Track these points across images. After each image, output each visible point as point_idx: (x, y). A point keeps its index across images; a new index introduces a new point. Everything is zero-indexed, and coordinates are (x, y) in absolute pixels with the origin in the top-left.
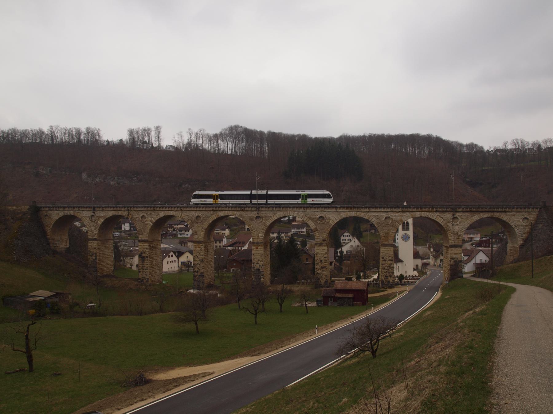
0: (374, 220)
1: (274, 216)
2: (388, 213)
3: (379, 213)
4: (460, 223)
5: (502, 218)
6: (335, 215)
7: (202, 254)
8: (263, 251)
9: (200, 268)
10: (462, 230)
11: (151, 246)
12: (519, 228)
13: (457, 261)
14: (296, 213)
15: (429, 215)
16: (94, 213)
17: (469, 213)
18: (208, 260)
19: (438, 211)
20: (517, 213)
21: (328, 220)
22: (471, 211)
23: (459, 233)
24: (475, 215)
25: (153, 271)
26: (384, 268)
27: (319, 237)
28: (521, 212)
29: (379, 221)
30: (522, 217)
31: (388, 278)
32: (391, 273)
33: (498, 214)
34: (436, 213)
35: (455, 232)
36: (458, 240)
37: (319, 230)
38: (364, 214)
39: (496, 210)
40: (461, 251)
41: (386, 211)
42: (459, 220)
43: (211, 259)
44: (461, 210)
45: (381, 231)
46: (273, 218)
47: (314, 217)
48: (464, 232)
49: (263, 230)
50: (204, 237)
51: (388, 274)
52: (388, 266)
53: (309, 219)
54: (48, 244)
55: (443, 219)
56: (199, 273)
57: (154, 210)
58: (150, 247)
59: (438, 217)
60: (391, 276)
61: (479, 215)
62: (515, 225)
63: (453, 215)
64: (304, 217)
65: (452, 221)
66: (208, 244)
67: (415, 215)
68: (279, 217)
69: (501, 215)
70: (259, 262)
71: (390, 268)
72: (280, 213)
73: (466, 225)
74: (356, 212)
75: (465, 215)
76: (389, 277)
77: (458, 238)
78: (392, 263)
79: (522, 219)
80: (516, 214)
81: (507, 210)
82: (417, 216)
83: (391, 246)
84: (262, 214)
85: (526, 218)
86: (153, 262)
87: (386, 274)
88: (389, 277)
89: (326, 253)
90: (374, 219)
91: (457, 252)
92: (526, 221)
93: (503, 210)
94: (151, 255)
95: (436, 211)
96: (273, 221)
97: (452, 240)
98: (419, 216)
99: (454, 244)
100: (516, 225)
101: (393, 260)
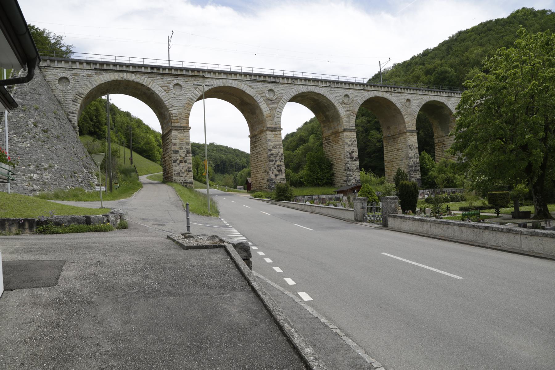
66: (443, 138)
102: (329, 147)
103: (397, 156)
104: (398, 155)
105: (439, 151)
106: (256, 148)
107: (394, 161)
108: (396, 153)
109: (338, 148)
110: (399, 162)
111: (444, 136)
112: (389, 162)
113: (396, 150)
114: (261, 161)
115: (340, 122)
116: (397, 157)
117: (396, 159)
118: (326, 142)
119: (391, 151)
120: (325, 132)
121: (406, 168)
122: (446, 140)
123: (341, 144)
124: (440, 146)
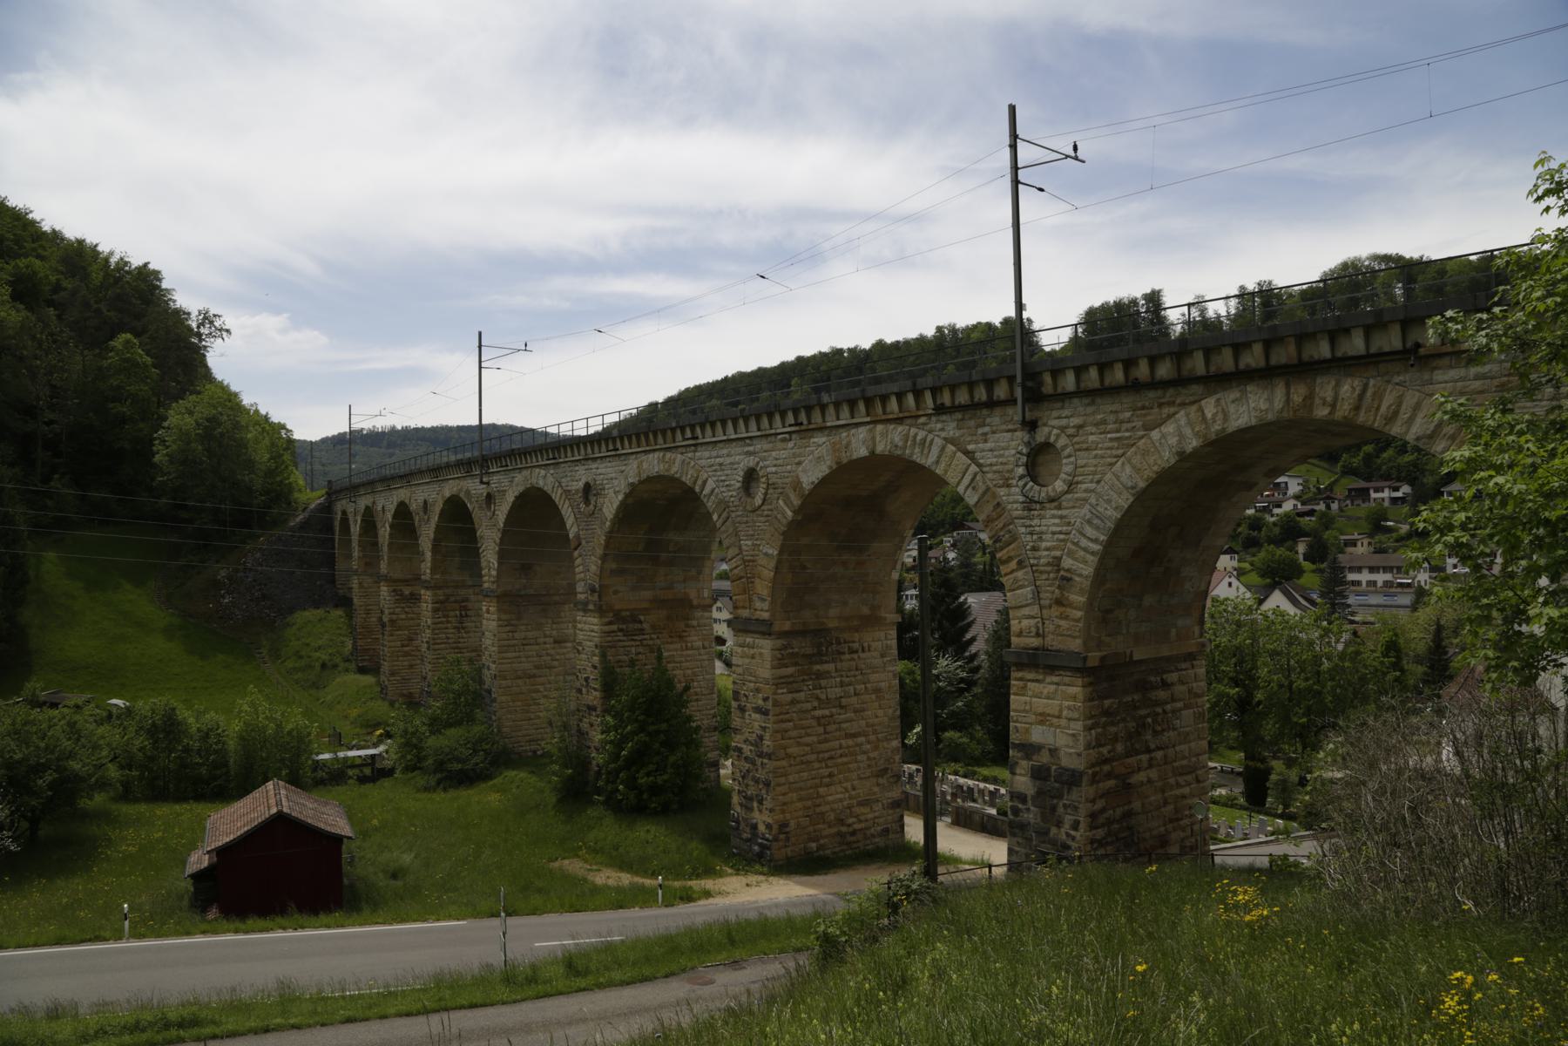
2: (751, 449)
3: (725, 451)
4: (1071, 486)
5: (1392, 417)
6: (613, 475)
8: (494, 623)
10: (1084, 542)
11: (407, 593)
14: (543, 472)
15: (907, 436)
17: (1128, 399)
22: (1134, 386)
23: (1067, 563)
24: (1166, 411)
25: (411, 666)
26: (739, 750)
31: (750, 809)
33: (1348, 388)
34: (939, 426)
35: (1044, 557)
36: (1061, 617)
37: (583, 542)
38: (684, 461)
39: (1323, 350)
40: (1074, 698)
48: (1093, 553)
50: (434, 569)
52: (752, 745)
53: (564, 497)
54: (333, 582)
55: (980, 465)
58: (401, 595)
59: (951, 448)
60: (761, 802)
61: (1194, 408)
63: (1031, 426)
65: (1021, 471)
66: (462, 592)
67: (848, 445)
68: (516, 493)
69: (1378, 396)
71: (759, 756)
72: (519, 477)
73: (1109, 501)
74: (662, 454)
75: (1104, 422)
77: (1059, 602)
78: (764, 729)
82: (854, 457)
86: (411, 640)
87: (747, 785)
88: (755, 804)
90: (707, 491)
91: (1052, 706)
94: (402, 619)
95: (940, 410)
97: (1026, 611)
98: (863, 452)
99: (1035, 642)
101: (765, 713)
102: (633, 650)
104: (558, 657)
105: (447, 628)
106: (824, 683)
107: (540, 676)
108: (552, 652)
109: (682, 656)
110: (561, 678)
111: (470, 586)
112: (520, 678)
113: (547, 640)
114: (854, 736)
115: (700, 573)
116: (556, 663)
117: (550, 668)
118: (621, 630)
119: (532, 641)
120: (616, 592)
122: (472, 597)
123: (700, 644)
124: (452, 613)
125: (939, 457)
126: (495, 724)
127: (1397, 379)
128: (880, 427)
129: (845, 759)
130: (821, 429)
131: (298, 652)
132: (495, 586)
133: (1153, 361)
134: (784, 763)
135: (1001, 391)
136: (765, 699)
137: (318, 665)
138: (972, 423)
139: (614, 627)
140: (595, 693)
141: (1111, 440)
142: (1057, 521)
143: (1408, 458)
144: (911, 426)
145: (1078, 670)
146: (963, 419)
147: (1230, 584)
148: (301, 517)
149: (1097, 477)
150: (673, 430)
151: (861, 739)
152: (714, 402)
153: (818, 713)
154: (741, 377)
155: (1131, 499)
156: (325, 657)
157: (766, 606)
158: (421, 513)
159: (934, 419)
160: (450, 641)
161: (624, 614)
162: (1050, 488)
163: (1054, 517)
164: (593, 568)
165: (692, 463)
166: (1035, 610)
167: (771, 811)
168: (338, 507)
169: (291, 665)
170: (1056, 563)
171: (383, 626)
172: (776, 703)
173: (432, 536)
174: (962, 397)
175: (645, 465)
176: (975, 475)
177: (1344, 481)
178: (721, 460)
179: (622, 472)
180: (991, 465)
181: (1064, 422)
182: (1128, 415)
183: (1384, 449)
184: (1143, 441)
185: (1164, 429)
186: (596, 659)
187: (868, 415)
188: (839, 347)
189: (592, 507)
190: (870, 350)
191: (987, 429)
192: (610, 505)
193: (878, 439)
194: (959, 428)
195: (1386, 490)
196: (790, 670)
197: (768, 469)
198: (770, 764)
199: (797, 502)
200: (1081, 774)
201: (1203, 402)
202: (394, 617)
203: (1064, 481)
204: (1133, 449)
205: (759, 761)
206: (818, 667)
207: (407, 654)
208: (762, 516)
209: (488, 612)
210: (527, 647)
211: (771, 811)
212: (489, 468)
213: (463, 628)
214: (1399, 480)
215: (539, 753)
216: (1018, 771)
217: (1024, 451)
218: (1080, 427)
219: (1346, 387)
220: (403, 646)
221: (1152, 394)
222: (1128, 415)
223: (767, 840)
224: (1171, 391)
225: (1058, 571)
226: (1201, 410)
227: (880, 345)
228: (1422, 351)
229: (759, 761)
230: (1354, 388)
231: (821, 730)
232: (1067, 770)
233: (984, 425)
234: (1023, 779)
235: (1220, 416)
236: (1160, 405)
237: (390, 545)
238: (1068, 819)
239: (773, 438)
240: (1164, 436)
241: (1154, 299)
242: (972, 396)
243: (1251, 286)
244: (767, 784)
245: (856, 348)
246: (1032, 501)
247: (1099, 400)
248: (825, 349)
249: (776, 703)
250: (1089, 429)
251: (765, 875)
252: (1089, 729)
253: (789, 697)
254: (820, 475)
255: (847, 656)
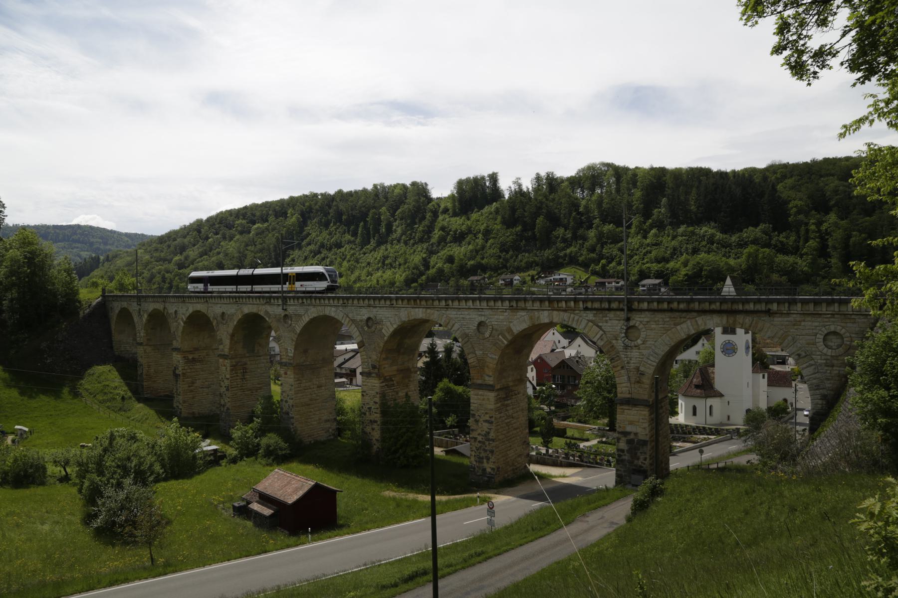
0: (456, 329)
1: (306, 315)
2: (483, 313)
3: (466, 313)
6: (390, 316)
7: (228, 376)
8: (292, 380)
9: (226, 401)
10: (649, 362)
11: (190, 358)
12: (812, 362)
13: (636, 440)
14: (333, 309)
15: (569, 317)
16: (140, 305)
17: (669, 314)
18: (243, 388)
19: (591, 309)
20: (809, 319)
21: (381, 326)
22: (671, 310)
23: (642, 369)
24: (682, 320)
25: (193, 398)
26: (476, 439)
27: (366, 360)
28: (821, 314)
29: (467, 331)
30: (824, 329)
32: (488, 452)
34: (585, 315)
35: (632, 366)
37: (366, 345)
39: (740, 307)
40: (645, 415)
41: (479, 309)
42: (643, 335)
43: (259, 384)
44: (645, 305)
45: (468, 354)
46: (304, 319)
47: (359, 318)
49: (292, 340)
50: (230, 349)
51: (483, 454)
53: (351, 322)
54: (112, 347)
55: (603, 331)
56: (225, 408)
57: (184, 302)
58: (188, 359)
59: (591, 324)
60: (488, 459)
61: (693, 320)
62: (798, 352)
64: (344, 318)
65: (623, 335)
67: (538, 318)
70: (288, 400)
74: (424, 310)
76: (485, 461)
77: (638, 382)
78: (491, 429)
79: (822, 337)
80: (804, 321)
81: (774, 307)
82: (542, 322)
83: (490, 390)
84: (291, 310)
85: (835, 333)
86: (193, 383)
88: (485, 461)
89: (377, 393)
90: (455, 328)
92: (834, 341)
93: (762, 307)
95: (586, 309)
96: (304, 324)
97: (624, 385)
98: (546, 321)
99: (629, 396)
100: (803, 354)
101: (491, 423)
102: (390, 394)
103: (317, 396)
105: (237, 379)
108: (316, 392)
114: (515, 429)
116: (318, 398)
117: (316, 400)
118: (386, 385)
120: (384, 368)
121: (331, 413)
122: (249, 363)
124: (239, 371)
125: (585, 327)
126: (292, 430)
127: (762, 319)
128: (555, 313)
129: (513, 439)
130: (523, 309)
131: (103, 390)
132: (292, 361)
133: (679, 303)
134: (497, 443)
135: (614, 305)
136: (491, 417)
137: (119, 398)
138: (601, 315)
139: (384, 384)
140: (376, 415)
141: (661, 327)
142: (638, 354)
143: (622, 267)
144: (571, 313)
145: (646, 406)
146: (596, 314)
147: (554, 334)
148: (88, 310)
149: (655, 340)
150: (433, 300)
151: (518, 430)
152: (240, 221)
153: (507, 421)
154: (255, 207)
155: (668, 348)
156: (122, 393)
157: (491, 379)
158: (219, 319)
159: (582, 312)
160: (239, 386)
161: (387, 378)
162: (635, 342)
163: (636, 352)
164: (374, 357)
165: (445, 316)
166: (629, 385)
167: (494, 463)
168: (117, 306)
169: (101, 398)
170: (638, 369)
171: (176, 376)
172: (495, 418)
173: (231, 331)
174: (597, 305)
175: (412, 313)
176: (602, 335)
177: (592, 277)
178: (464, 316)
179: (396, 315)
180: (609, 331)
181: (642, 319)
182: (668, 319)
183: (610, 262)
184: (673, 330)
185: (681, 325)
186: (377, 400)
187: (549, 307)
188: (315, 192)
189: (373, 329)
190: (334, 195)
191: (608, 318)
192: (388, 329)
193: (554, 317)
194: (594, 317)
195: (613, 284)
196: (499, 405)
197: (493, 323)
198: (494, 444)
199: (510, 338)
200: (648, 441)
201: (697, 319)
202: (184, 371)
203: (641, 340)
204: (670, 332)
205: (487, 443)
206: (506, 402)
207: (191, 391)
208: (488, 341)
209: (286, 374)
210: (306, 391)
211: (494, 463)
212: (286, 302)
213: (244, 379)
214: (618, 278)
215: (312, 442)
216: (621, 441)
217: (625, 328)
218: (648, 322)
219: (747, 320)
220: (189, 387)
221: (677, 314)
222: (668, 319)
223: (492, 475)
224: (684, 314)
225: (638, 371)
226: (696, 321)
227: (340, 192)
228: (771, 311)
229: (487, 443)
230: (749, 320)
231: (507, 428)
232: (641, 440)
233: (606, 317)
234: (623, 444)
235: (703, 324)
236: (680, 318)
237: (183, 332)
238: (642, 457)
239: (496, 310)
240: (681, 328)
241: (494, 178)
242: (601, 306)
243: (543, 174)
244: (492, 452)
245: (325, 193)
246: (627, 346)
247: (656, 313)
248: (307, 193)
249: (495, 418)
250: (652, 323)
251: (494, 489)
252: (649, 425)
253: (499, 416)
254: (523, 328)
255: (514, 397)
